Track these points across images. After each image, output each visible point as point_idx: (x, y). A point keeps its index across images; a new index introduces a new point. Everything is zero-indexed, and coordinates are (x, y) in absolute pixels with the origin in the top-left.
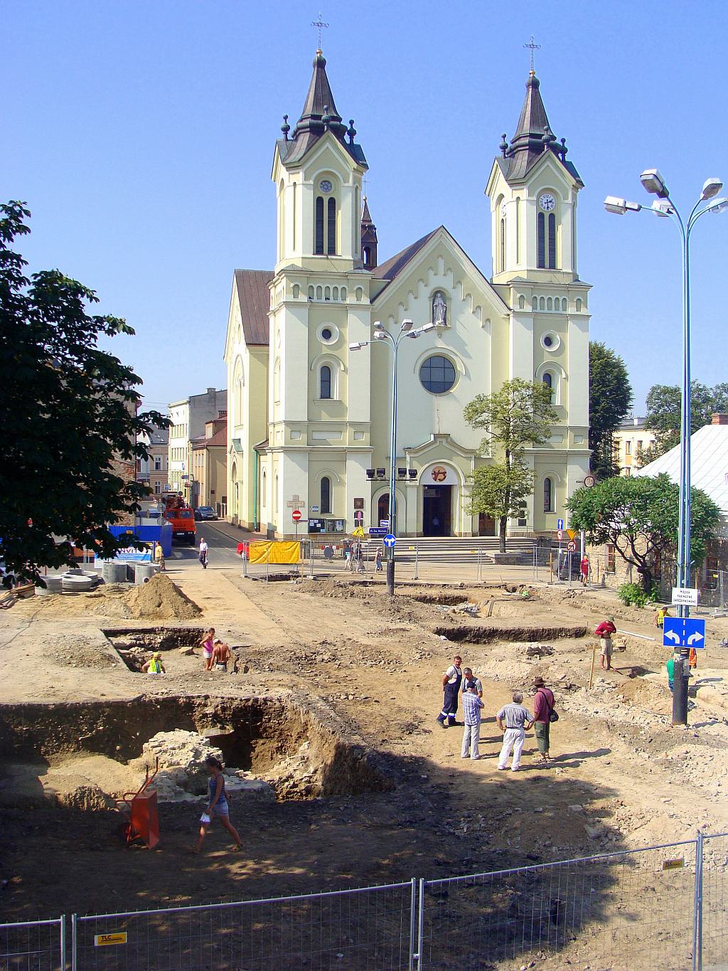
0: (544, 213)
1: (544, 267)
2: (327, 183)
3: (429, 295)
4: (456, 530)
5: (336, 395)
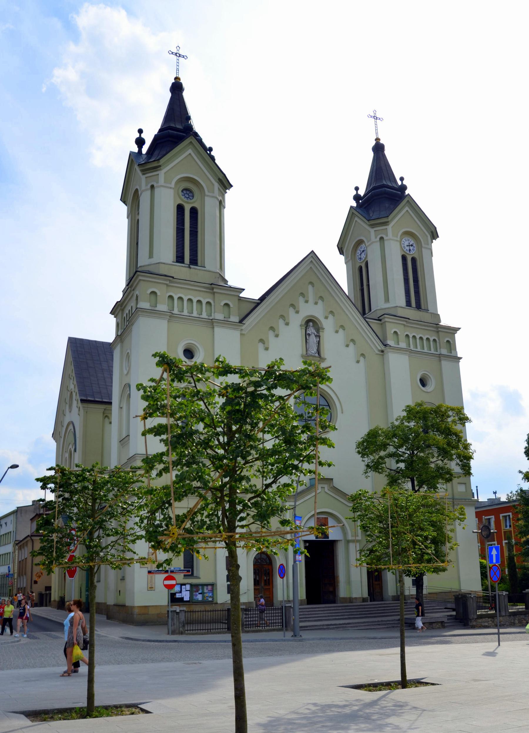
2: (188, 192)
3: (299, 323)
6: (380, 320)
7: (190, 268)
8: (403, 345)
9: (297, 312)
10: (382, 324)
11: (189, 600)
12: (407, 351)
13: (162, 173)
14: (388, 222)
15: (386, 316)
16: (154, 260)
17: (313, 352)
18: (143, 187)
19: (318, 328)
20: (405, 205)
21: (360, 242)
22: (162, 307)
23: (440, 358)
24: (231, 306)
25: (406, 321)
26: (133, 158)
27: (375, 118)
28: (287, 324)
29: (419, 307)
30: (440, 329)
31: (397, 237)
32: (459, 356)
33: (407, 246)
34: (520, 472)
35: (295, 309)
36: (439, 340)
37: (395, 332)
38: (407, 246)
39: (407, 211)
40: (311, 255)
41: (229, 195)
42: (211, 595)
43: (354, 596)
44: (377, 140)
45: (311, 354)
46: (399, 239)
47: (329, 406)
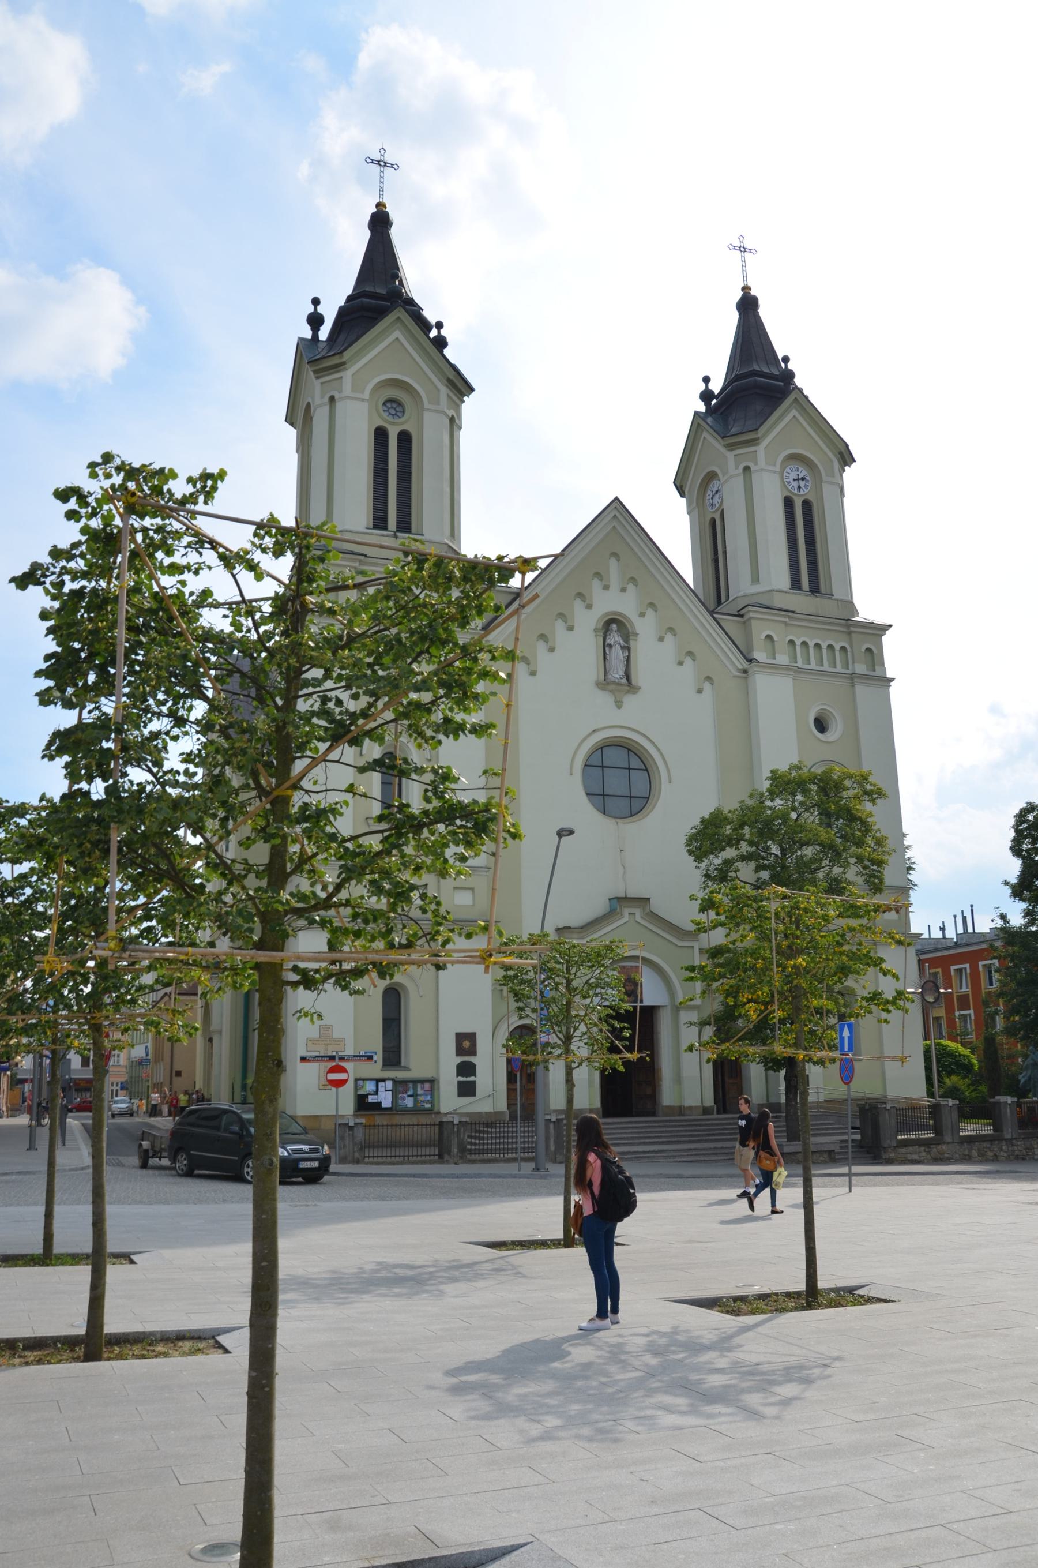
0: (793, 497)
2: (394, 405)
4: (668, 1097)
6: (742, 616)
7: (396, 537)
8: (783, 659)
9: (589, 607)
10: (744, 623)
11: (390, 1106)
12: (792, 669)
13: (347, 375)
14: (758, 439)
15: (750, 608)
17: (617, 676)
19: (627, 634)
20: (789, 407)
21: (711, 476)
23: (852, 679)
25: (789, 617)
26: (304, 347)
27: (742, 249)
28: (571, 628)
29: (815, 589)
30: (852, 629)
31: (775, 465)
32: (889, 676)
33: (794, 480)
34: (1006, 883)
35: (584, 601)
36: (852, 647)
37: (769, 637)
38: (794, 480)
39: (794, 416)
40: (614, 505)
41: (469, 406)
42: (429, 1098)
43: (688, 1103)
44: (746, 289)
45: (613, 679)
46: (778, 469)
47: (646, 769)
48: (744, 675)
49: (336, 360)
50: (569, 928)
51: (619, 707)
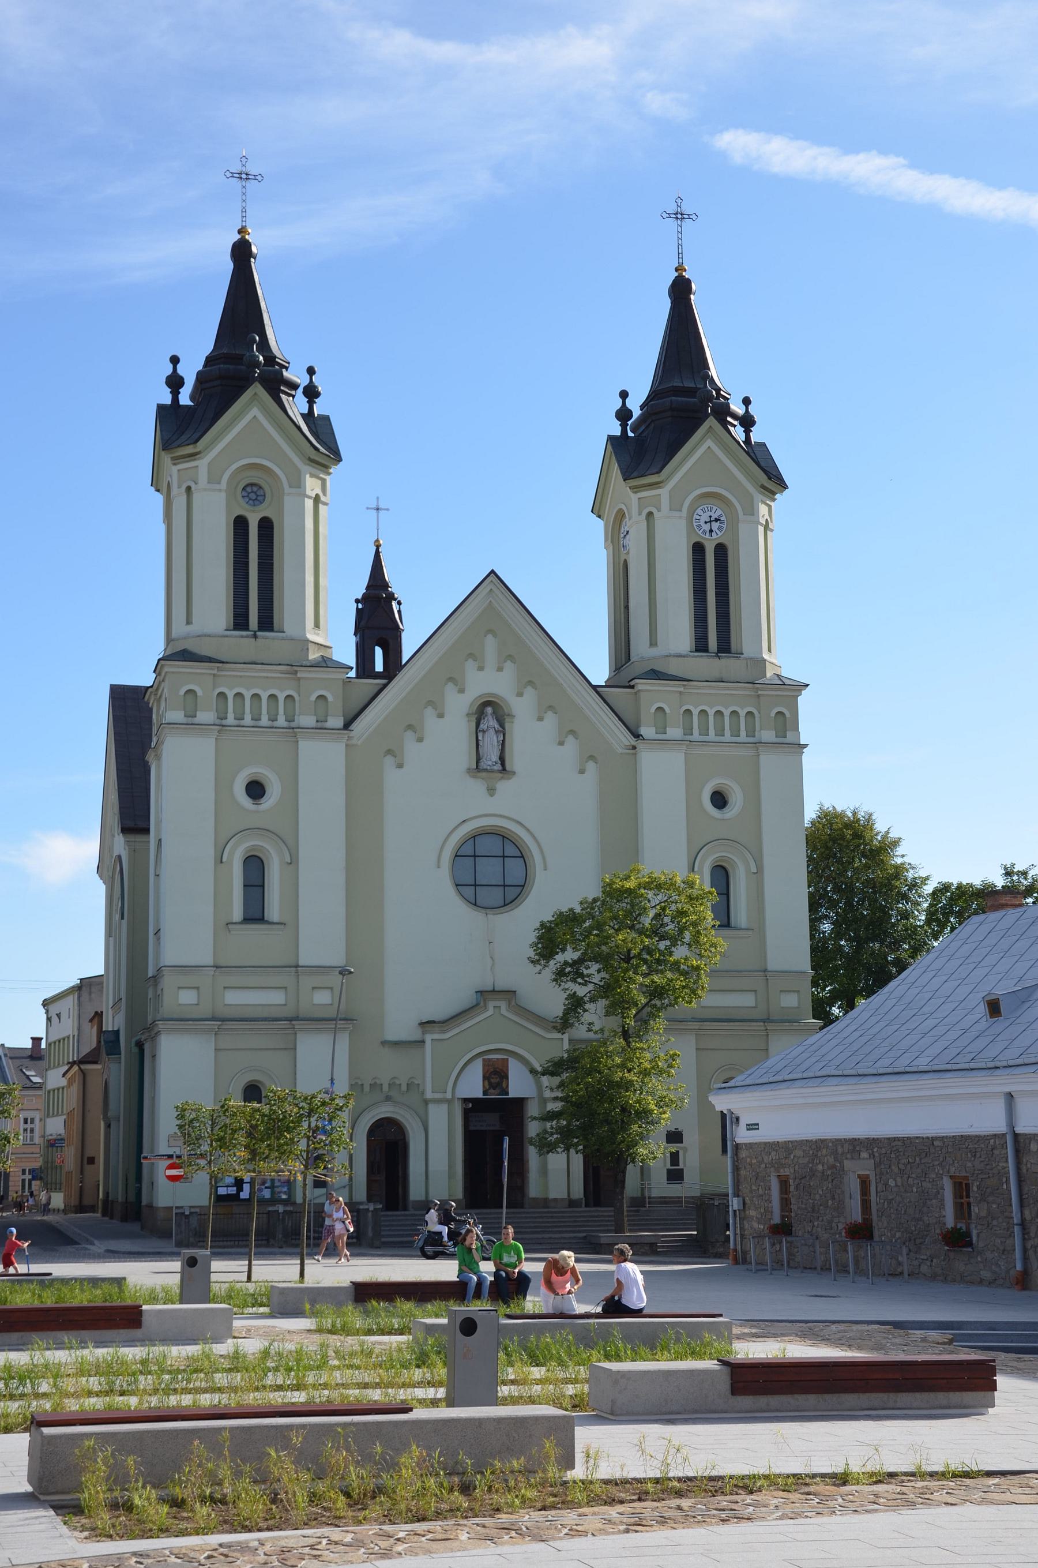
0: (703, 541)
1: (706, 650)
2: (255, 489)
5: (274, 910)
6: (632, 687)
7: (255, 636)
9: (462, 691)
10: (636, 693)
11: (248, 1197)
13: (202, 464)
16: (195, 628)
17: (490, 763)
18: (175, 490)
22: (206, 716)
24: (330, 698)
30: (760, 692)
33: (706, 523)
37: (660, 709)
38: (706, 523)
40: (492, 577)
42: (285, 1189)
43: (552, 1195)
45: (485, 767)
46: (684, 512)
47: (522, 857)
48: (633, 751)
49: (189, 450)
50: (433, 1022)
51: (492, 795)
